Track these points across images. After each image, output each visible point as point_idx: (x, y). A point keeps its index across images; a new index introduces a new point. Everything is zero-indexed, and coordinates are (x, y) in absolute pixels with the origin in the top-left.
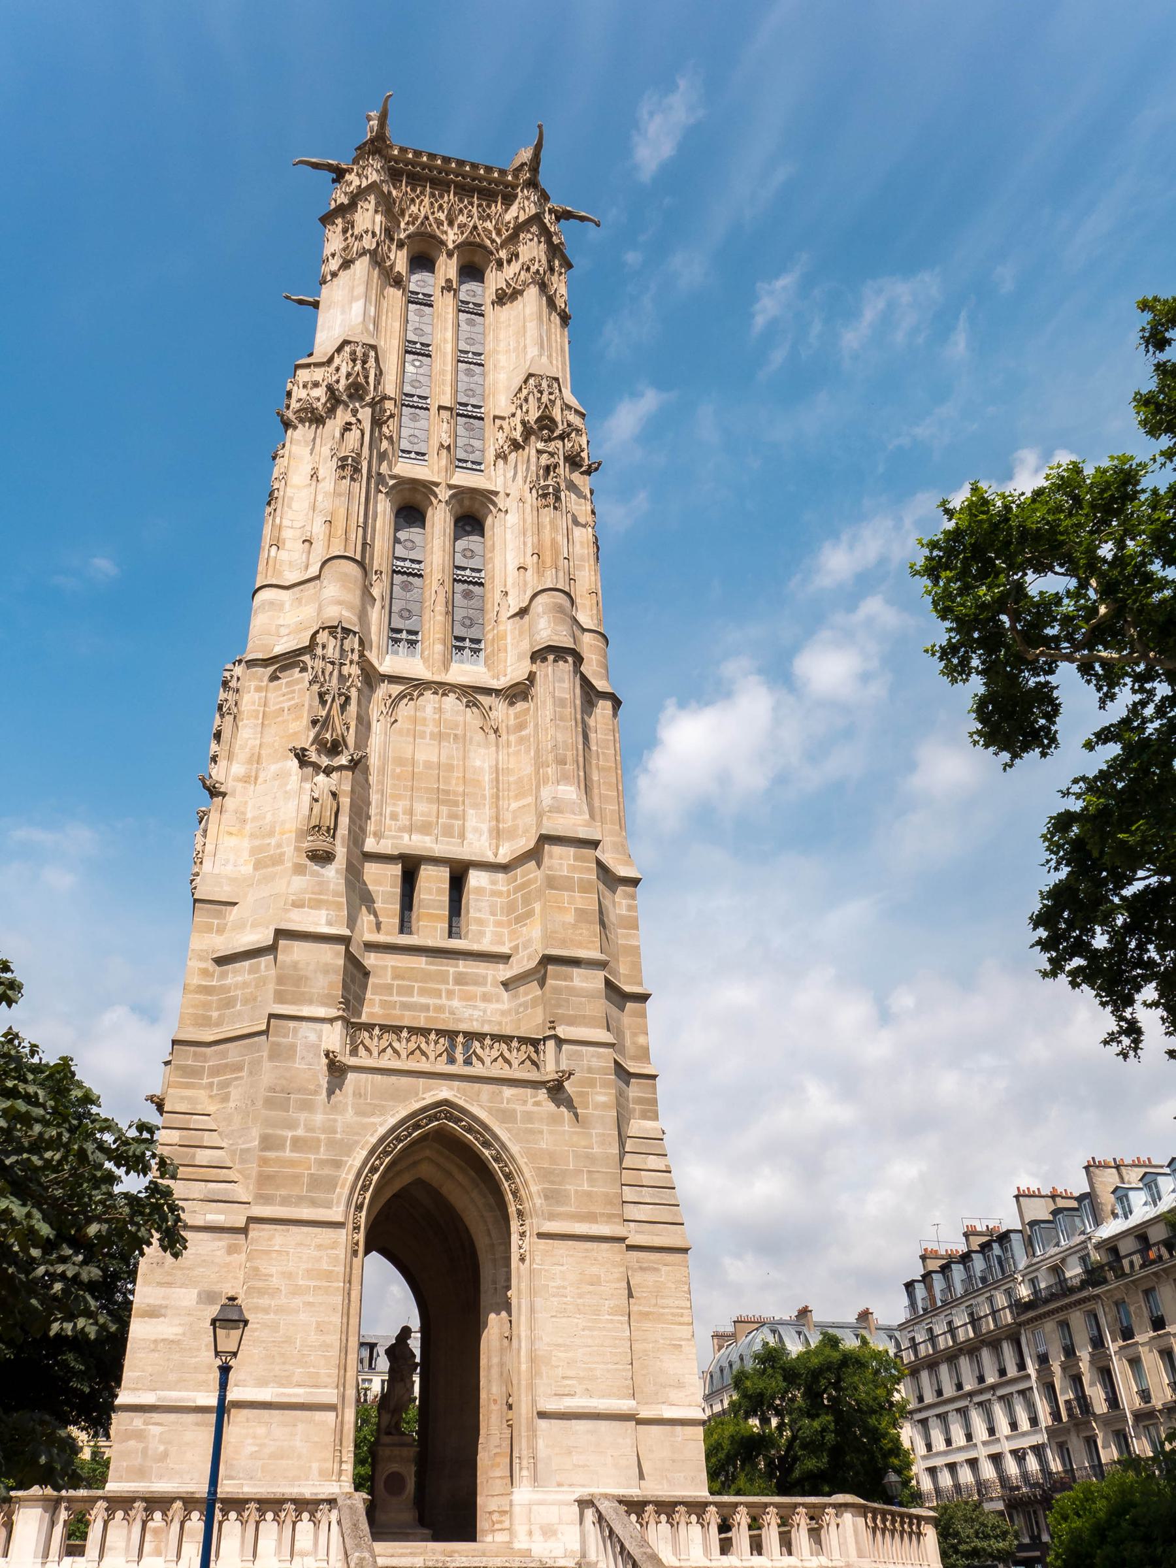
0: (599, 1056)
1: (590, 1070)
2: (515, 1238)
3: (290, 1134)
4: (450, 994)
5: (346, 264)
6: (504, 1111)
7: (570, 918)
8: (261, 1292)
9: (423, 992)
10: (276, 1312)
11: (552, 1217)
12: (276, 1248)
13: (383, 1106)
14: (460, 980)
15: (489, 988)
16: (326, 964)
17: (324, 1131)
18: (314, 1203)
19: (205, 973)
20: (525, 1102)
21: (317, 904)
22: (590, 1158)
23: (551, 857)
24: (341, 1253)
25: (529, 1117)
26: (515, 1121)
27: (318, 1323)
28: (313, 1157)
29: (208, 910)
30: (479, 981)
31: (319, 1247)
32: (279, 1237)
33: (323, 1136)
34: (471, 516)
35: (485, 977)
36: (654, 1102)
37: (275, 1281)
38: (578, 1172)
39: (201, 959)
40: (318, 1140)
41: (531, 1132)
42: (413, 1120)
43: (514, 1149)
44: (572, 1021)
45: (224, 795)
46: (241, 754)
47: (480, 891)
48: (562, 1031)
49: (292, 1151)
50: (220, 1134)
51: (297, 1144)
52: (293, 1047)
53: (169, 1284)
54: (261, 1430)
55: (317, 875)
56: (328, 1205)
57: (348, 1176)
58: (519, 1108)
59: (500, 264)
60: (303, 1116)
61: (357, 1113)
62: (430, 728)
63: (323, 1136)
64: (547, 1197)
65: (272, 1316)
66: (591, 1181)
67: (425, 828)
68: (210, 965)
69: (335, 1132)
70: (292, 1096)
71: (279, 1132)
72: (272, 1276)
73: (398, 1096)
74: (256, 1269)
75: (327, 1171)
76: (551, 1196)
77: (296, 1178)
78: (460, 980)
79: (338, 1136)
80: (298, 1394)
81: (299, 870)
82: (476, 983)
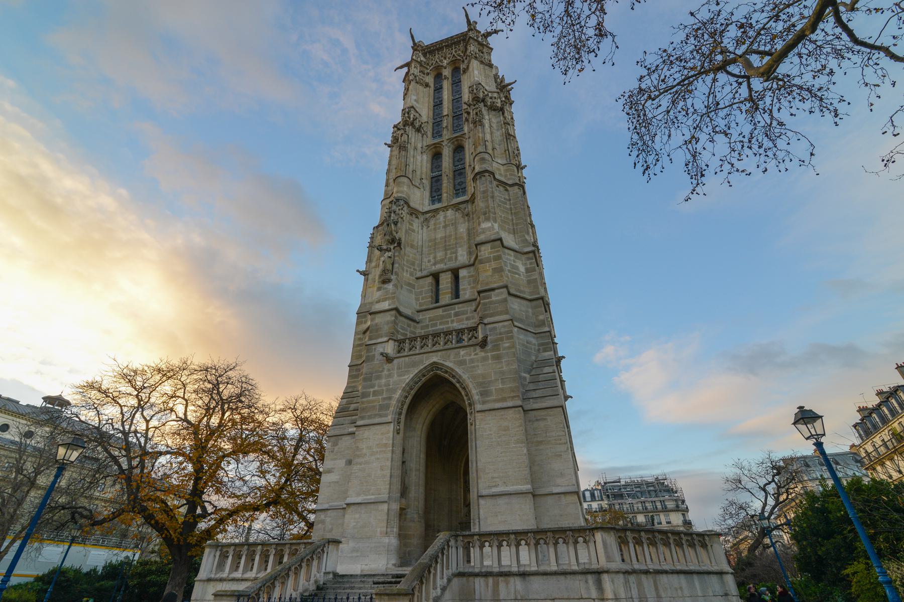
0: (504, 326)
1: (501, 334)
4: (452, 321)
7: (490, 273)
8: (358, 456)
9: (441, 324)
11: (484, 403)
14: (456, 314)
15: (469, 315)
17: (385, 386)
18: (381, 416)
21: (385, 300)
22: (503, 373)
24: (391, 435)
25: (472, 361)
30: (463, 313)
32: (366, 433)
35: (467, 311)
38: (497, 380)
41: (474, 367)
43: (465, 377)
44: (492, 315)
46: (375, 259)
47: (464, 277)
48: (486, 321)
51: (375, 393)
53: (335, 459)
54: (357, 516)
56: (386, 416)
57: (394, 402)
58: (468, 358)
60: (377, 382)
62: (443, 224)
64: (481, 395)
66: (503, 383)
67: (442, 261)
68: (361, 336)
73: (414, 365)
75: (386, 402)
76: (484, 394)
77: (374, 407)
78: (456, 314)
80: (371, 498)
81: (379, 289)
82: (463, 314)
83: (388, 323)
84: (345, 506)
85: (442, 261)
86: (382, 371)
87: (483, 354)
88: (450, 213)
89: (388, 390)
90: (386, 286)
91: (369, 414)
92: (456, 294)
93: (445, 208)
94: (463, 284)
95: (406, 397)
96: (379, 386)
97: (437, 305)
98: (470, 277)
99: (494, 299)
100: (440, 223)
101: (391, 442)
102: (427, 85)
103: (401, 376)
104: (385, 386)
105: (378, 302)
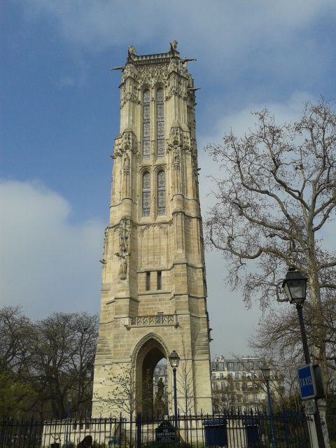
5: (125, 103)
9: (152, 304)
18: (125, 358)
19: (104, 307)
21: (123, 291)
34: (160, 170)
42: (145, 338)
44: (181, 310)
59: (166, 87)
73: (141, 332)
81: (119, 283)
85: (151, 263)
87: (175, 331)
88: (156, 228)
90: (123, 281)
92: (159, 287)
93: (154, 225)
94: (164, 281)
96: (123, 342)
97: (149, 292)
98: (169, 277)
99: (181, 300)
105: (119, 291)
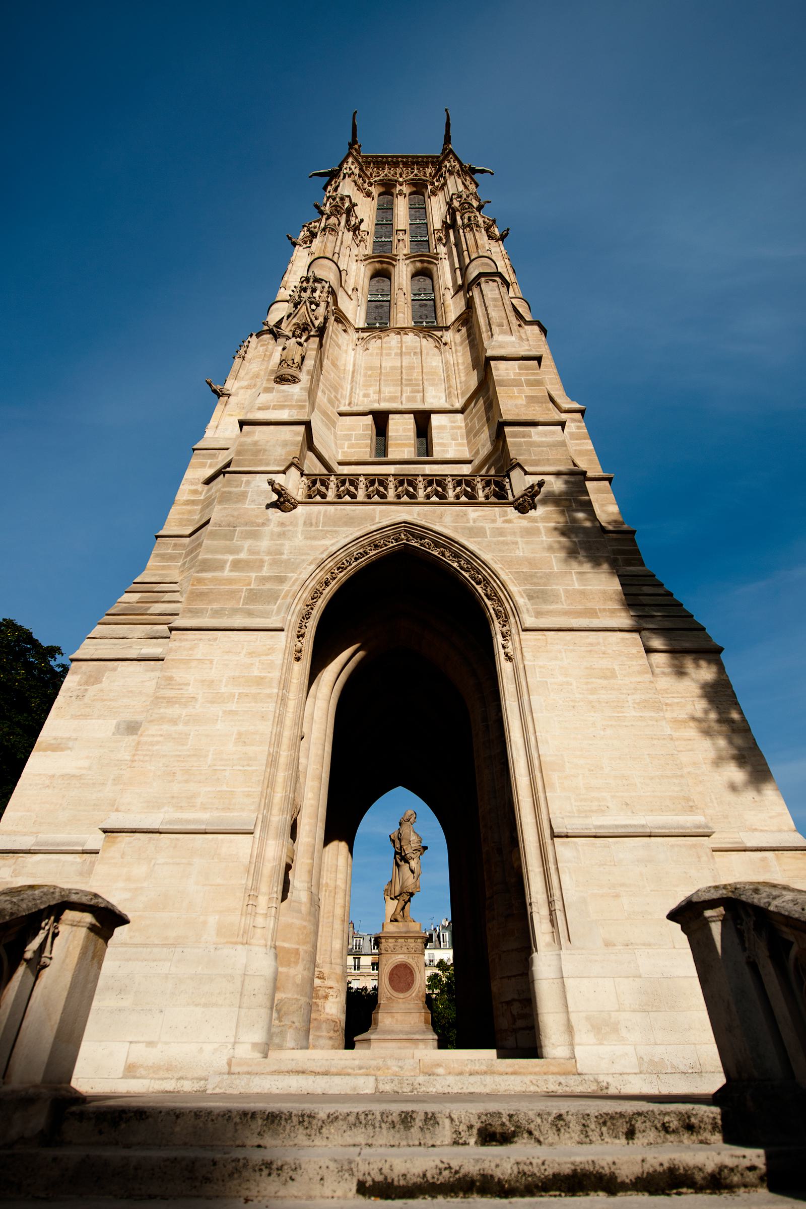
2: (499, 640)
3: (231, 558)
6: (471, 529)
7: (522, 401)
8: (171, 702)
10: (186, 723)
12: (199, 656)
13: (336, 532)
16: (285, 441)
17: (269, 553)
18: (250, 614)
20: (494, 521)
21: (282, 407)
23: (497, 369)
24: (278, 658)
25: (501, 532)
26: (485, 535)
27: (240, 734)
28: (253, 575)
29: (203, 455)
31: (251, 654)
32: (202, 644)
33: (266, 558)
36: (637, 552)
37: (191, 690)
39: (192, 484)
40: (262, 561)
42: (371, 540)
45: (229, 395)
49: (231, 571)
50: (181, 594)
52: (244, 495)
53: (85, 716)
55: (283, 391)
56: (266, 615)
58: (488, 526)
60: (247, 544)
61: (306, 538)
63: (266, 558)
64: (530, 597)
65: (180, 727)
69: (282, 554)
70: (238, 529)
71: (219, 557)
72: (188, 684)
73: (350, 521)
74: (171, 678)
75: (268, 586)
77: (232, 594)
79: (285, 557)
83: (285, 444)
84: (96, 840)
86: (263, 524)
89: (274, 563)
90: (285, 387)
91: (215, 606)
95: (327, 583)
100: (390, 348)
101: (276, 674)
102: (369, 194)
103: (314, 538)
104: (269, 553)
